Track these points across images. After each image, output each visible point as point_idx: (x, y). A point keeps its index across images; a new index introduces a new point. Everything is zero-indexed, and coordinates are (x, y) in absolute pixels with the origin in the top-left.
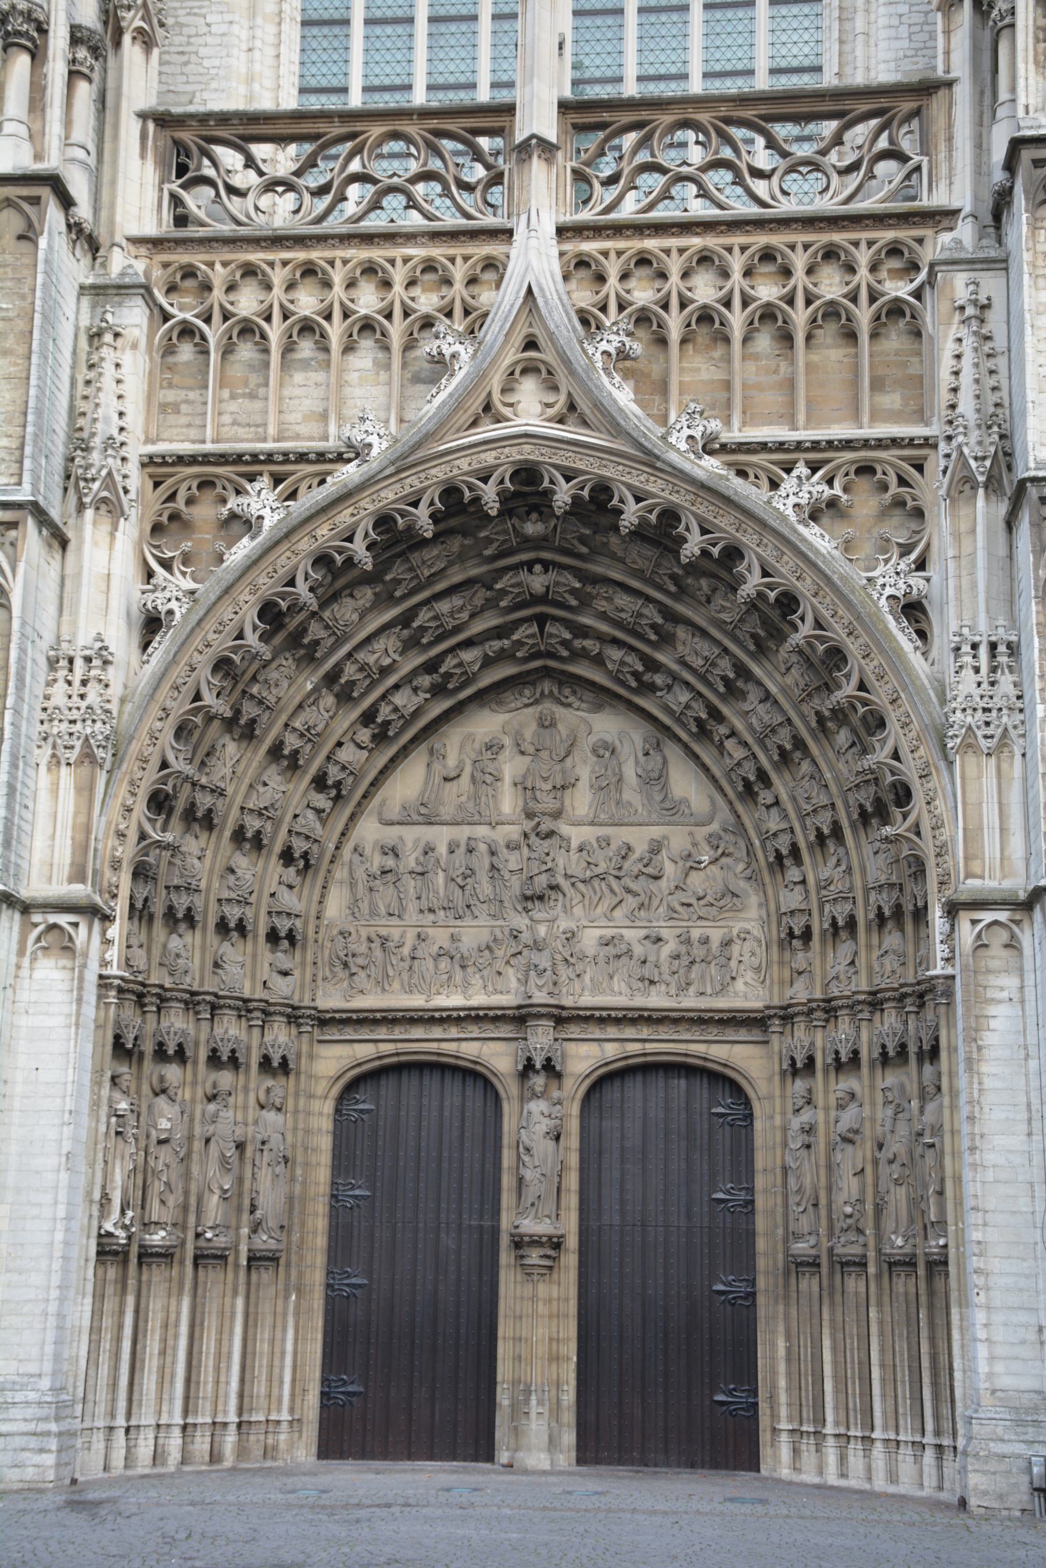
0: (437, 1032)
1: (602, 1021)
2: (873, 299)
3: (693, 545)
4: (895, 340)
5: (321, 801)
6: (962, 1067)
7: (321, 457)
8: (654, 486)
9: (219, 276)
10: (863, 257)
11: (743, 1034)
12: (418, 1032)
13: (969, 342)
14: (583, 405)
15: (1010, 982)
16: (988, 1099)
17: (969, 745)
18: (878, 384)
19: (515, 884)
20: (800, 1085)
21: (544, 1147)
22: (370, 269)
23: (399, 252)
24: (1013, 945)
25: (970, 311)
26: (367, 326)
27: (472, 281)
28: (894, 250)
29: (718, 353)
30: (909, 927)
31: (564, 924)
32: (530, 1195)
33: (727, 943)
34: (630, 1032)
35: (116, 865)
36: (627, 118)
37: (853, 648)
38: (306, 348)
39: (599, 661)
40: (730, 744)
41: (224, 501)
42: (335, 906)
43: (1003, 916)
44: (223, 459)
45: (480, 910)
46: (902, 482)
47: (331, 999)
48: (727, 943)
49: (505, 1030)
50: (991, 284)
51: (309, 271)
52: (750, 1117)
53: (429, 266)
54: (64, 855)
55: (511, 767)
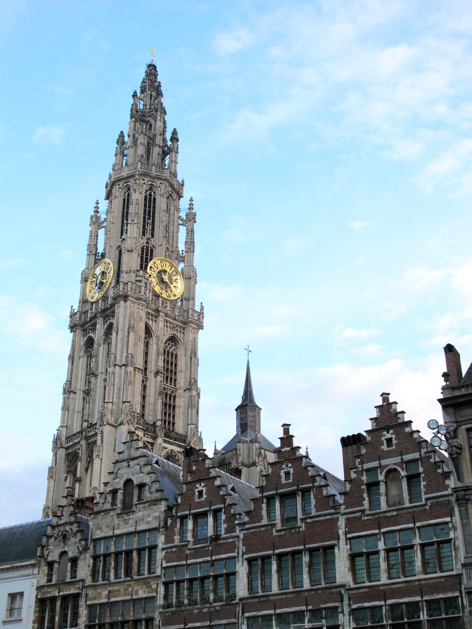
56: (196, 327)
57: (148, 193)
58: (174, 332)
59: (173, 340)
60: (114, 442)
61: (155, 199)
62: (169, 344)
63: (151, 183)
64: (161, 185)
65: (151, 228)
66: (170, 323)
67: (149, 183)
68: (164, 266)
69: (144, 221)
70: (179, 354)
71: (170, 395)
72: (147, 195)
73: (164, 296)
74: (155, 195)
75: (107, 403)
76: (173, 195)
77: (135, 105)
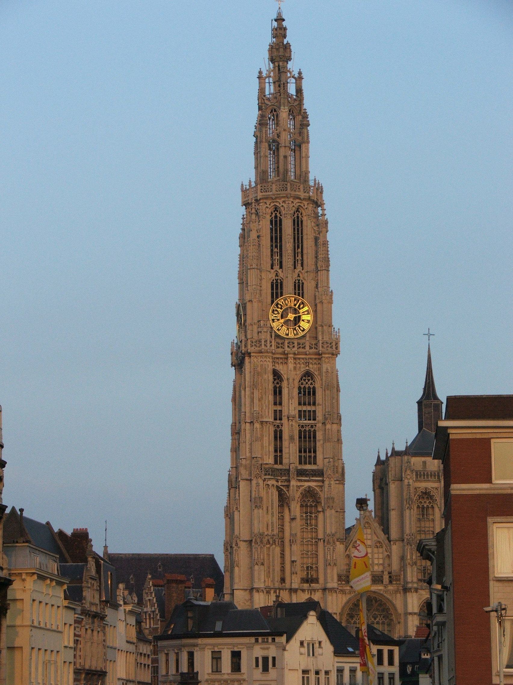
56: (330, 356)
57: (274, 215)
58: (307, 368)
59: (308, 375)
60: (250, 494)
61: (281, 220)
62: (305, 380)
63: (273, 204)
64: (283, 205)
65: (278, 258)
66: (303, 359)
67: (272, 204)
68: (289, 302)
69: (272, 251)
70: (316, 386)
71: (310, 431)
72: (272, 218)
73: (291, 335)
74: (281, 215)
75: (241, 459)
76: (302, 205)
77: (262, 91)
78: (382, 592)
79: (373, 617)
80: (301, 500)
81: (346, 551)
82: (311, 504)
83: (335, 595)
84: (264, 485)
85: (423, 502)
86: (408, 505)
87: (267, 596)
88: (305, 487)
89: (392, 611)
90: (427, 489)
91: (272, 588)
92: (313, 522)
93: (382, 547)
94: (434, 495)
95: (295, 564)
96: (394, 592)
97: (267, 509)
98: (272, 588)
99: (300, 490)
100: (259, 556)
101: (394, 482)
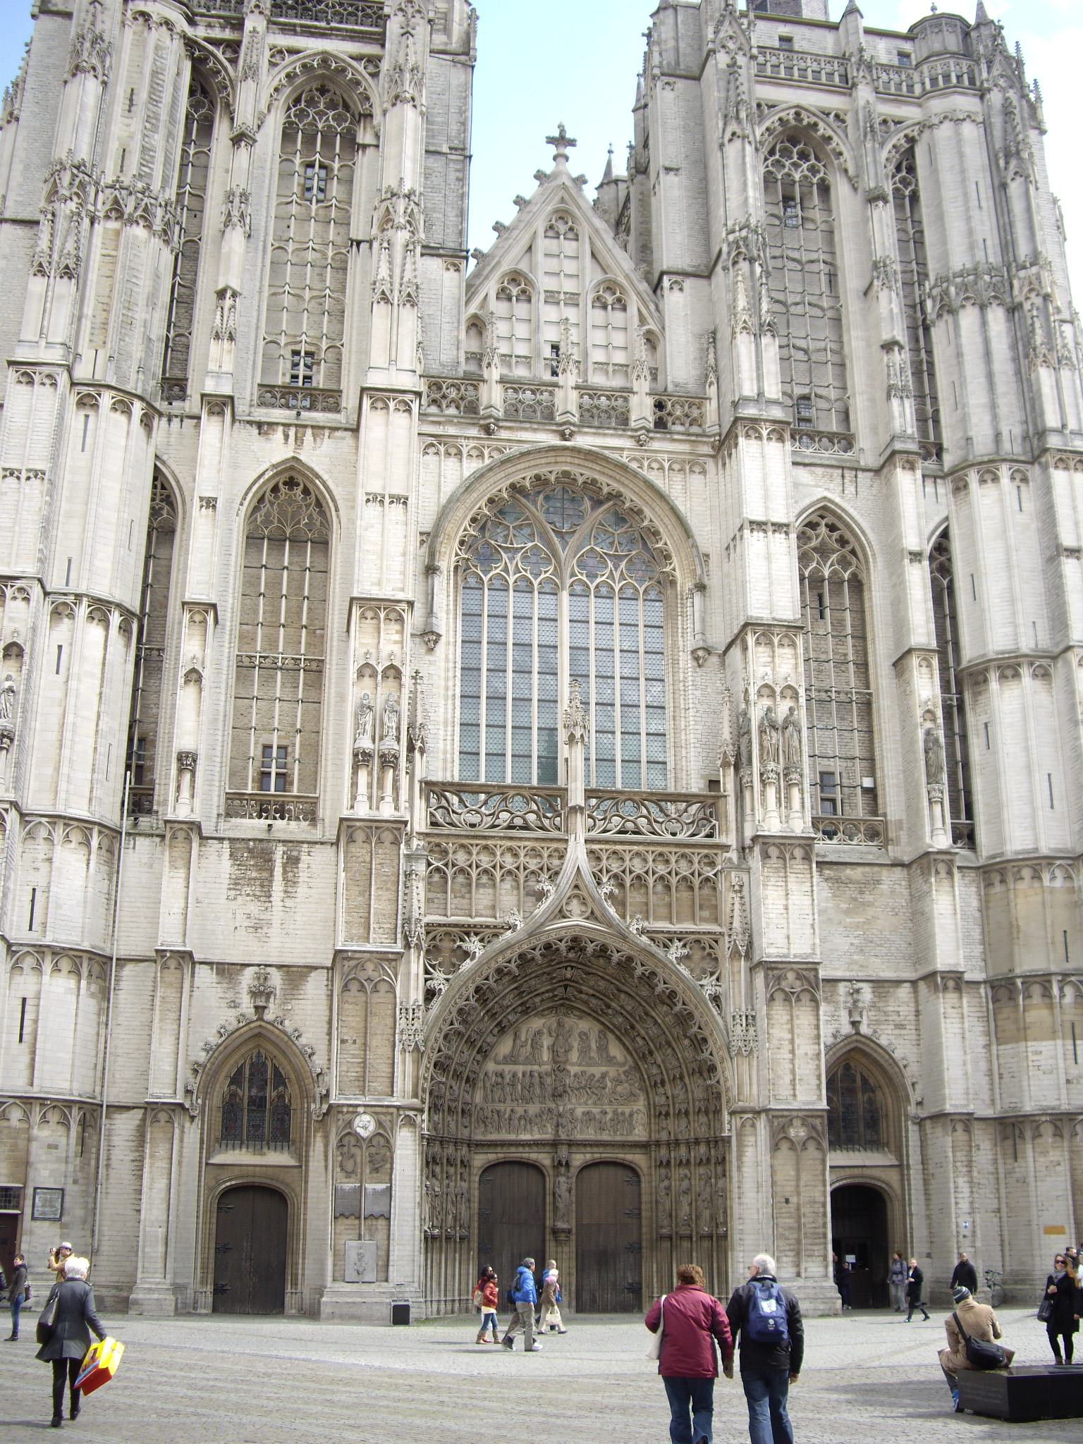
0: (521, 1149)
1: (585, 1145)
2: (700, 875)
3: (639, 970)
4: (706, 891)
5: (479, 1057)
6: (734, 1169)
7: (495, 927)
8: (625, 947)
9: (451, 848)
10: (696, 859)
11: (638, 1150)
12: (513, 1149)
13: (737, 900)
14: (597, 913)
15: (752, 1139)
16: (745, 1180)
17: (739, 1053)
18: (701, 908)
19: (549, 1089)
20: (663, 1171)
21: (565, 1194)
22: (510, 849)
23: (522, 844)
24: (753, 1126)
25: (737, 888)
26: (510, 872)
27: (550, 856)
28: (706, 856)
29: (643, 891)
30: (711, 1116)
31: (569, 1107)
32: (560, 1213)
33: (631, 1115)
34: (595, 1150)
35: (424, 1090)
36: (608, 795)
37: (696, 1013)
38: (485, 879)
39: (586, 1003)
40: (638, 1039)
41: (455, 941)
42: (478, 1097)
43: (750, 1116)
44: (456, 926)
45: (536, 1100)
46: (711, 947)
47: (479, 1137)
48: (631, 1115)
49: (548, 1149)
50: (745, 877)
51: (486, 847)
52: (639, 1181)
53: (533, 849)
54: (409, 1087)
55: (546, 1041)
78: (625, 460)
79: (581, 564)
80: (289, 108)
81: (467, 302)
82: (330, 127)
83: (400, 419)
84: (129, 14)
85: (787, 164)
86: (734, 126)
87: (82, 418)
88: (301, 55)
89: (669, 539)
90: (804, 114)
91: (109, 387)
92: (335, 189)
93: (624, 309)
94: (830, 138)
95: (228, 302)
96: (676, 467)
97: (131, 100)
98: (109, 387)
99: (284, 63)
100: (58, 242)
101: (671, 80)
